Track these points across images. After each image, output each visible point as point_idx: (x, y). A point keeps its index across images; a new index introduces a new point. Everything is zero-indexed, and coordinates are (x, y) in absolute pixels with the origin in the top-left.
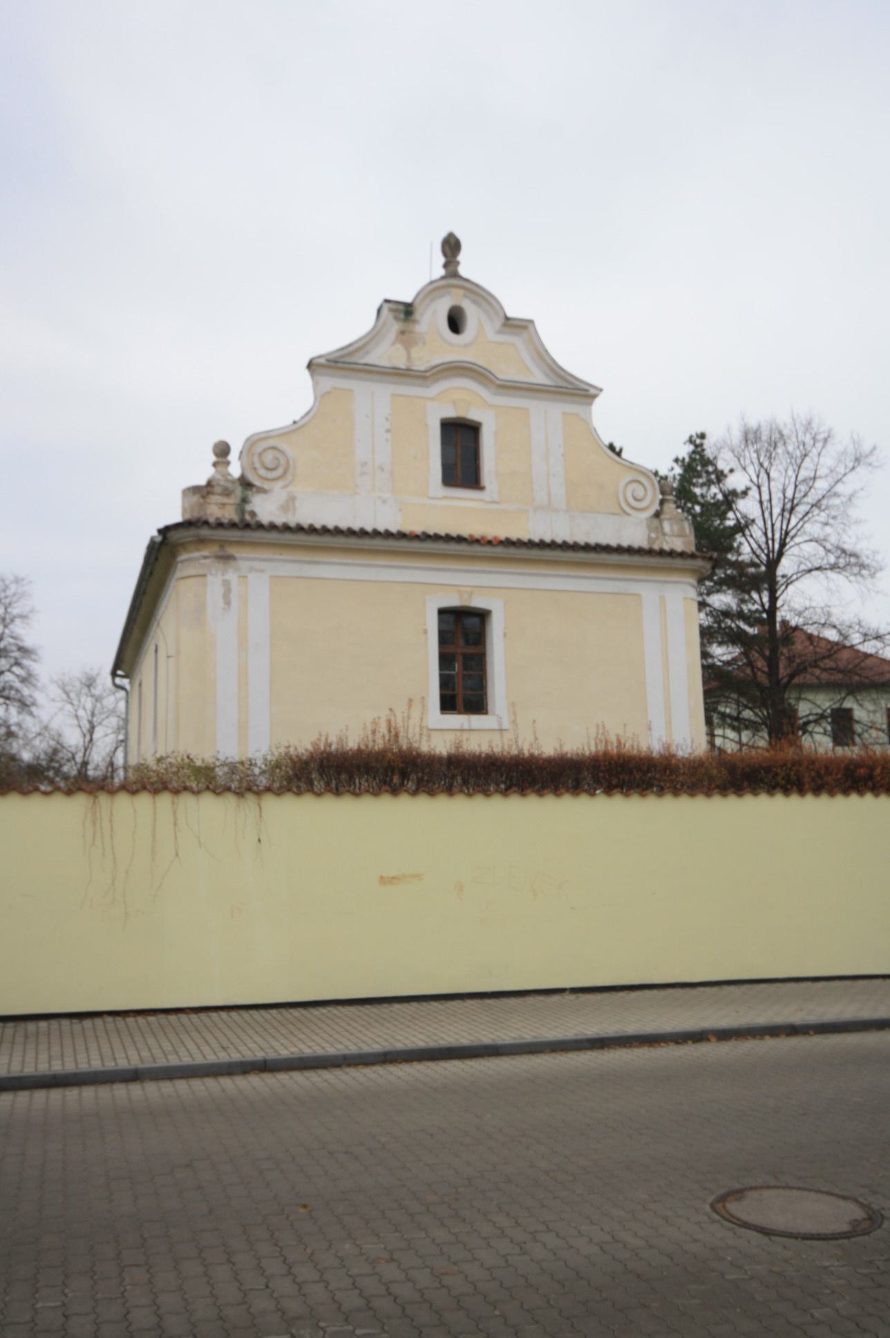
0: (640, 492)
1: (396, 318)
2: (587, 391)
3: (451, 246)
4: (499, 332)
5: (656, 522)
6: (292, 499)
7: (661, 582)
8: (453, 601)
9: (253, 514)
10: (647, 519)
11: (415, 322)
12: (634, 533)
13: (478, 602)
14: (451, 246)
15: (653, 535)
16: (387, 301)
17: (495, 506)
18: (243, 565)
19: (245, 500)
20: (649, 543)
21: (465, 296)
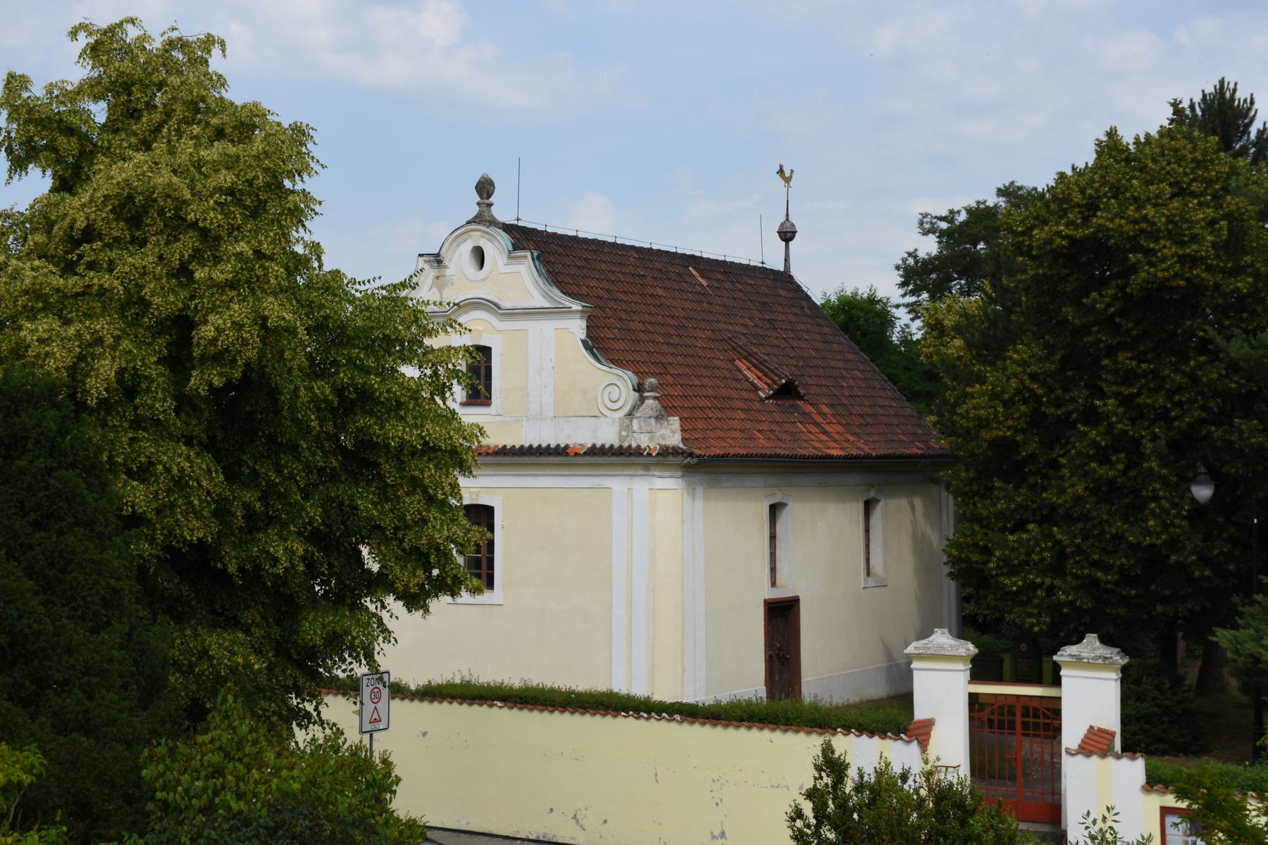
0: (615, 397)
1: (432, 267)
3: (485, 188)
7: (630, 475)
10: (620, 419)
11: (446, 267)
12: (608, 436)
14: (485, 188)
15: (624, 433)
16: (421, 255)
17: (498, 418)
20: (620, 441)
21: (483, 237)
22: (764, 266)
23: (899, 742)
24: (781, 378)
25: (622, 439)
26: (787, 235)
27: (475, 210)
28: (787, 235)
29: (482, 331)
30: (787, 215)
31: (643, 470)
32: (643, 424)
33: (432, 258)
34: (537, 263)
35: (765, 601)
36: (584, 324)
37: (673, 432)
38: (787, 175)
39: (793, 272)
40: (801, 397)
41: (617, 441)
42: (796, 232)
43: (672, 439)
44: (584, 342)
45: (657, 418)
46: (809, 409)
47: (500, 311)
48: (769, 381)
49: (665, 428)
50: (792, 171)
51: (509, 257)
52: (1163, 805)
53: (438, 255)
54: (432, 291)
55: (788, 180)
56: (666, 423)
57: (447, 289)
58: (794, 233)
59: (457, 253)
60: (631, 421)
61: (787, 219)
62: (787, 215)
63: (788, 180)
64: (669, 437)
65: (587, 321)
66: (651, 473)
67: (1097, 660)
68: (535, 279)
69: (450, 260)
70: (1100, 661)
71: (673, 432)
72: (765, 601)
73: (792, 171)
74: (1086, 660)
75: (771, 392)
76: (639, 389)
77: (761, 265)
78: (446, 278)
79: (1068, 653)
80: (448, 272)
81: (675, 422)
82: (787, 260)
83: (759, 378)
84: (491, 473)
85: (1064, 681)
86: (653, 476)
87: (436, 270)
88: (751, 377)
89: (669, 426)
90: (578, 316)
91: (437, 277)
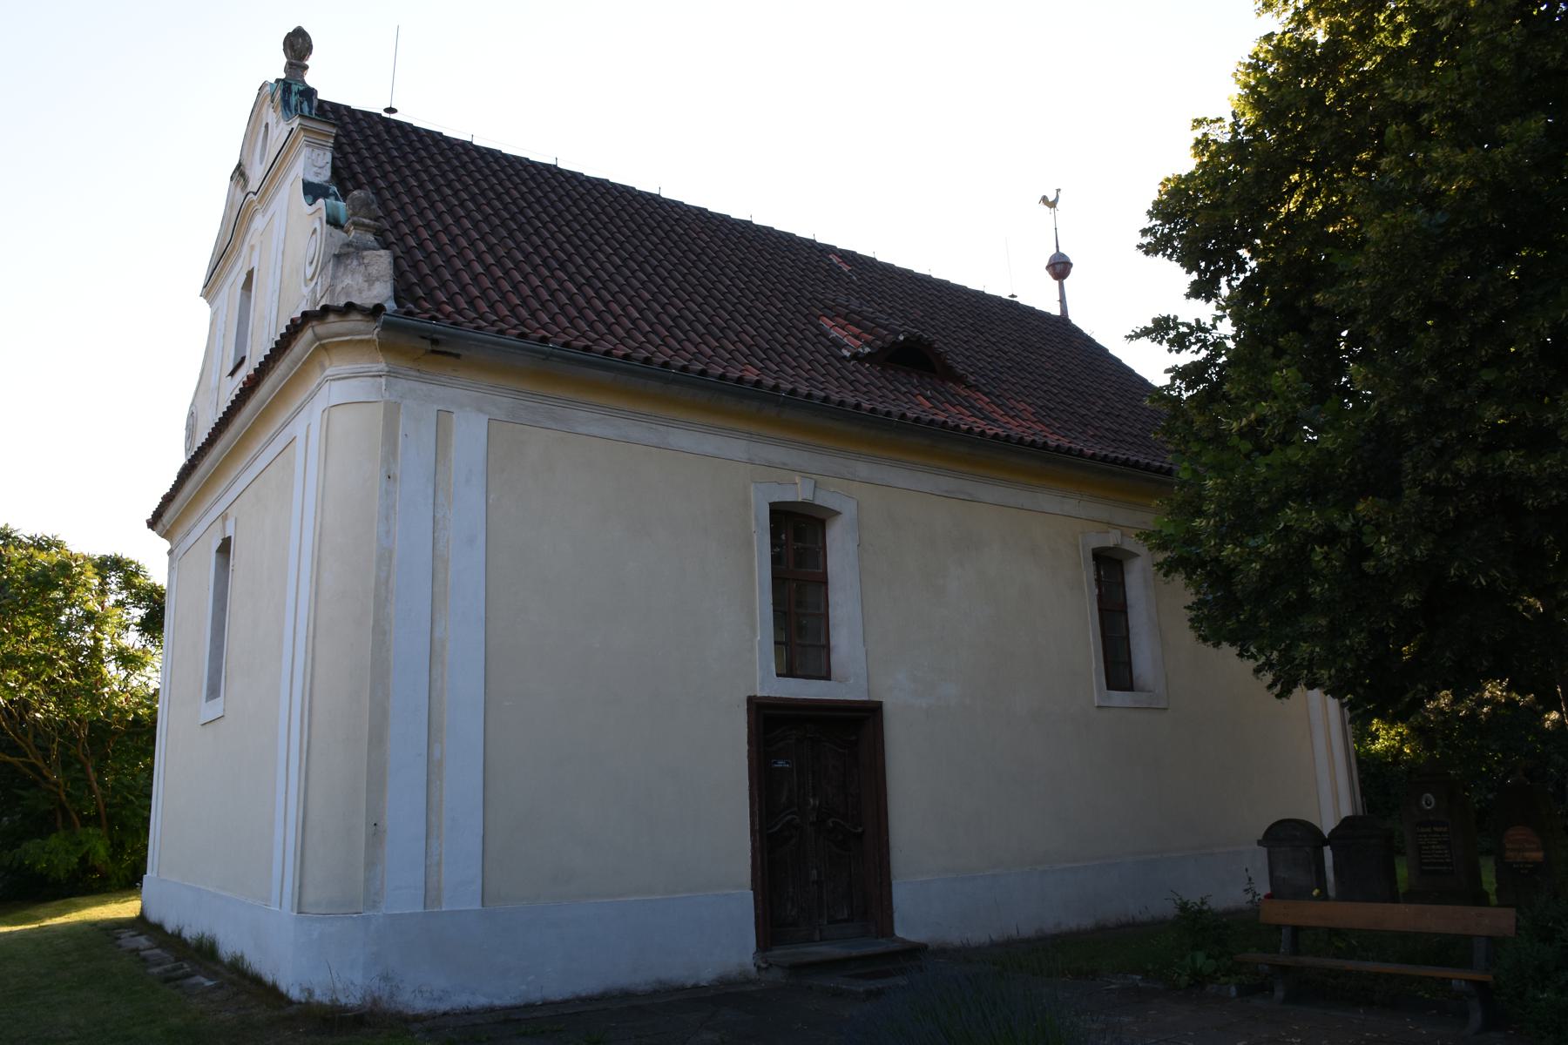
2: (292, 129)
3: (298, 45)
14: (298, 45)
22: (1015, 299)
26: (1060, 268)
28: (1060, 268)
30: (1057, 247)
35: (752, 701)
36: (326, 158)
37: (370, 280)
38: (1051, 199)
40: (959, 380)
53: (239, 165)
55: (1052, 205)
56: (355, 263)
61: (1058, 250)
62: (1057, 247)
64: (360, 291)
71: (370, 280)
72: (752, 701)
75: (867, 350)
82: (1063, 300)
88: (835, 333)
89: (362, 268)
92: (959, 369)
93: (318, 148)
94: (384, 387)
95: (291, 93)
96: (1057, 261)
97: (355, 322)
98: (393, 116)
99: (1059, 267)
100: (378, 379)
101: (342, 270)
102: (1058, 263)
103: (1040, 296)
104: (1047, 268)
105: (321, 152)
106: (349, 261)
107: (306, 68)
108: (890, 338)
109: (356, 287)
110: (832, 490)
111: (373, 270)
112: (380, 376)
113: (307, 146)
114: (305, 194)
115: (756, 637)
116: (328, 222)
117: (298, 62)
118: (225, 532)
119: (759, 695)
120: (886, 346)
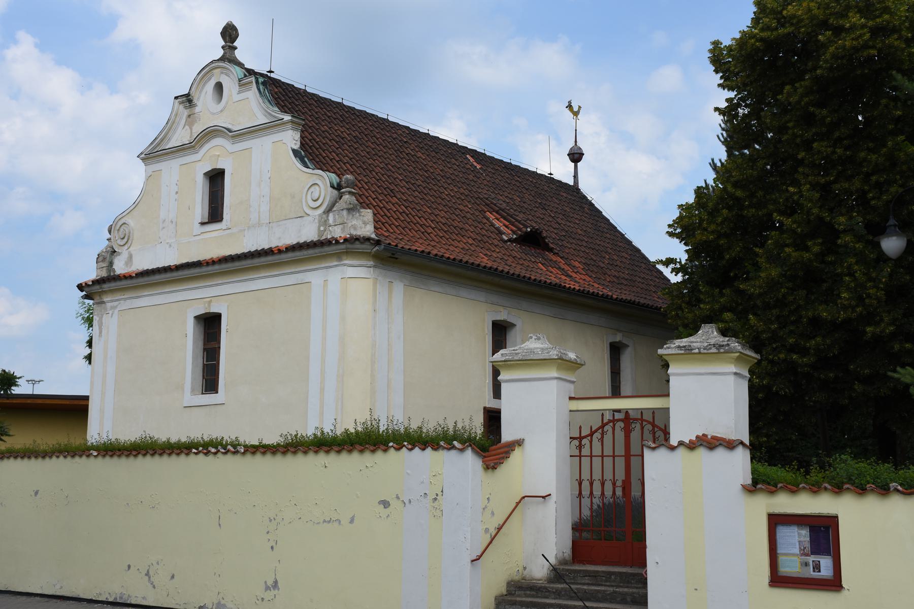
0: (316, 196)
2: (283, 119)
3: (230, 33)
4: (239, 92)
5: (324, 216)
6: (131, 257)
7: (327, 268)
8: (201, 311)
9: (114, 271)
10: (320, 215)
11: (195, 105)
12: (308, 232)
13: (214, 309)
14: (230, 33)
16: (176, 98)
18: (109, 305)
19: (111, 264)
21: (222, 73)
22: (552, 176)
23: (453, 452)
24: (527, 227)
25: (321, 233)
26: (576, 156)
27: (220, 53)
28: (576, 156)
29: (219, 156)
30: (576, 141)
31: (337, 261)
32: (337, 216)
33: (185, 99)
34: (261, 87)
35: (485, 408)
36: (297, 136)
37: (365, 223)
38: (576, 109)
39: (582, 186)
40: (551, 250)
41: (316, 236)
42: (583, 154)
43: (363, 230)
44: (294, 151)
45: (349, 210)
46: (554, 258)
47: (231, 134)
48: (514, 229)
49: (357, 218)
50: (580, 107)
51: (240, 86)
52: (771, 511)
53: (188, 95)
54: (185, 129)
55: (576, 114)
56: (358, 214)
57: (196, 124)
58: (581, 155)
59: (204, 91)
60: (328, 216)
61: (576, 144)
62: (576, 141)
63: (576, 114)
64: (361, 228)
65: (302, 131)
66: (342, 263)
67: (710, 349)
68: (258, 101)
69: (199, 98)
70: (714, 350)
71: (365, 223)
72: (485, 408)
73: (580, 107)
74: (697, 351)
75: (515, 236)
76: (338, 187)
77: (550, 176)
78: (196, 115)
79: (677, 344)
80: (197, 109)
81: (368, 214)
82: (576, 176)
83: (506, 226)
84: (220, 282)
85: (675, 383)
86: (345, 265)
87: (188, 110)
88: (497, 224)
89: (361, 218)
90: (289, 126)
91: (189, 116)
92: (551, 246)
93: (295, 130)
94: (372, 272)
95: (259, 84)
96: (576, 152)
97: (367, 247)
98: (272, 75)
99: (576, 156)
100: (370, 268)
101: (351, 216)
102: (576, 153)
103: (562, 172)
104: (568, 155)
105: (296, 132)
106: (354, 213)
107: (235, 48)
108: (524, 230)
109: (359, 226)
110: (513, 314)
111: (365, 219)
112: (370, 267)
113: (292, 129)
114: (296, 157)
115: (486, 381)
116: (331, 186)
117: (231, 45)
118: (209, 306)
119: (487, 406)
120: (522, 234)
